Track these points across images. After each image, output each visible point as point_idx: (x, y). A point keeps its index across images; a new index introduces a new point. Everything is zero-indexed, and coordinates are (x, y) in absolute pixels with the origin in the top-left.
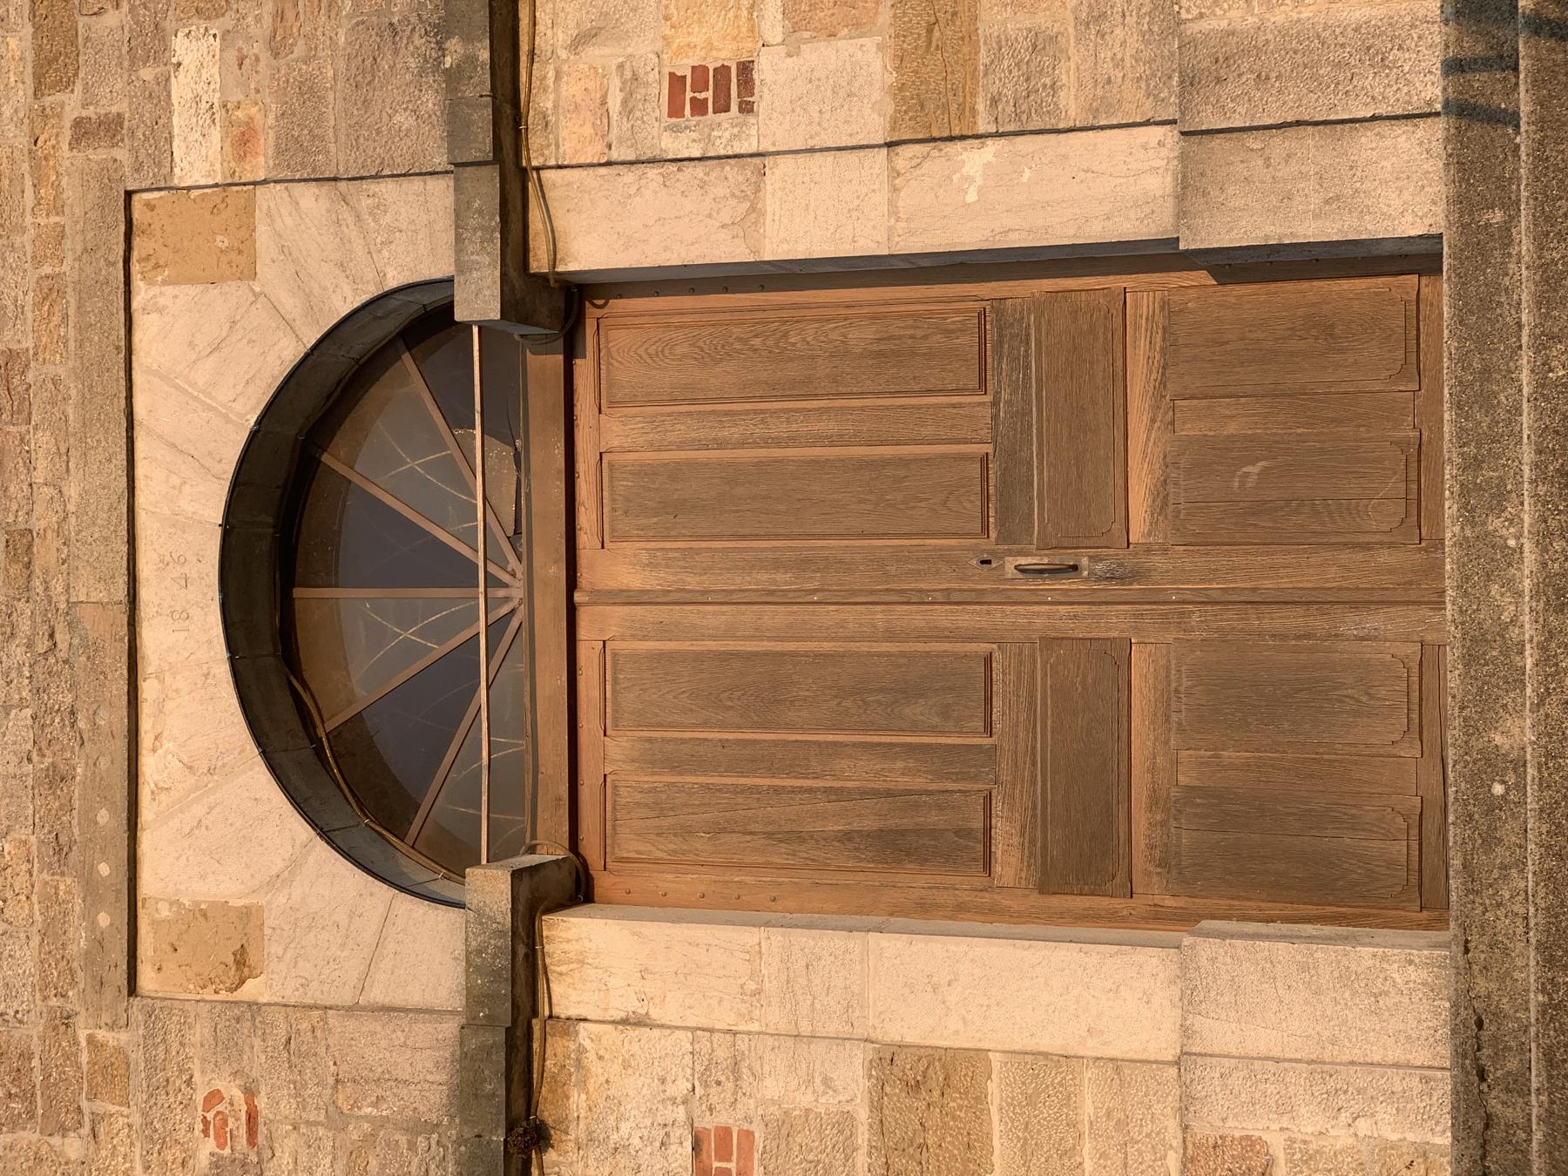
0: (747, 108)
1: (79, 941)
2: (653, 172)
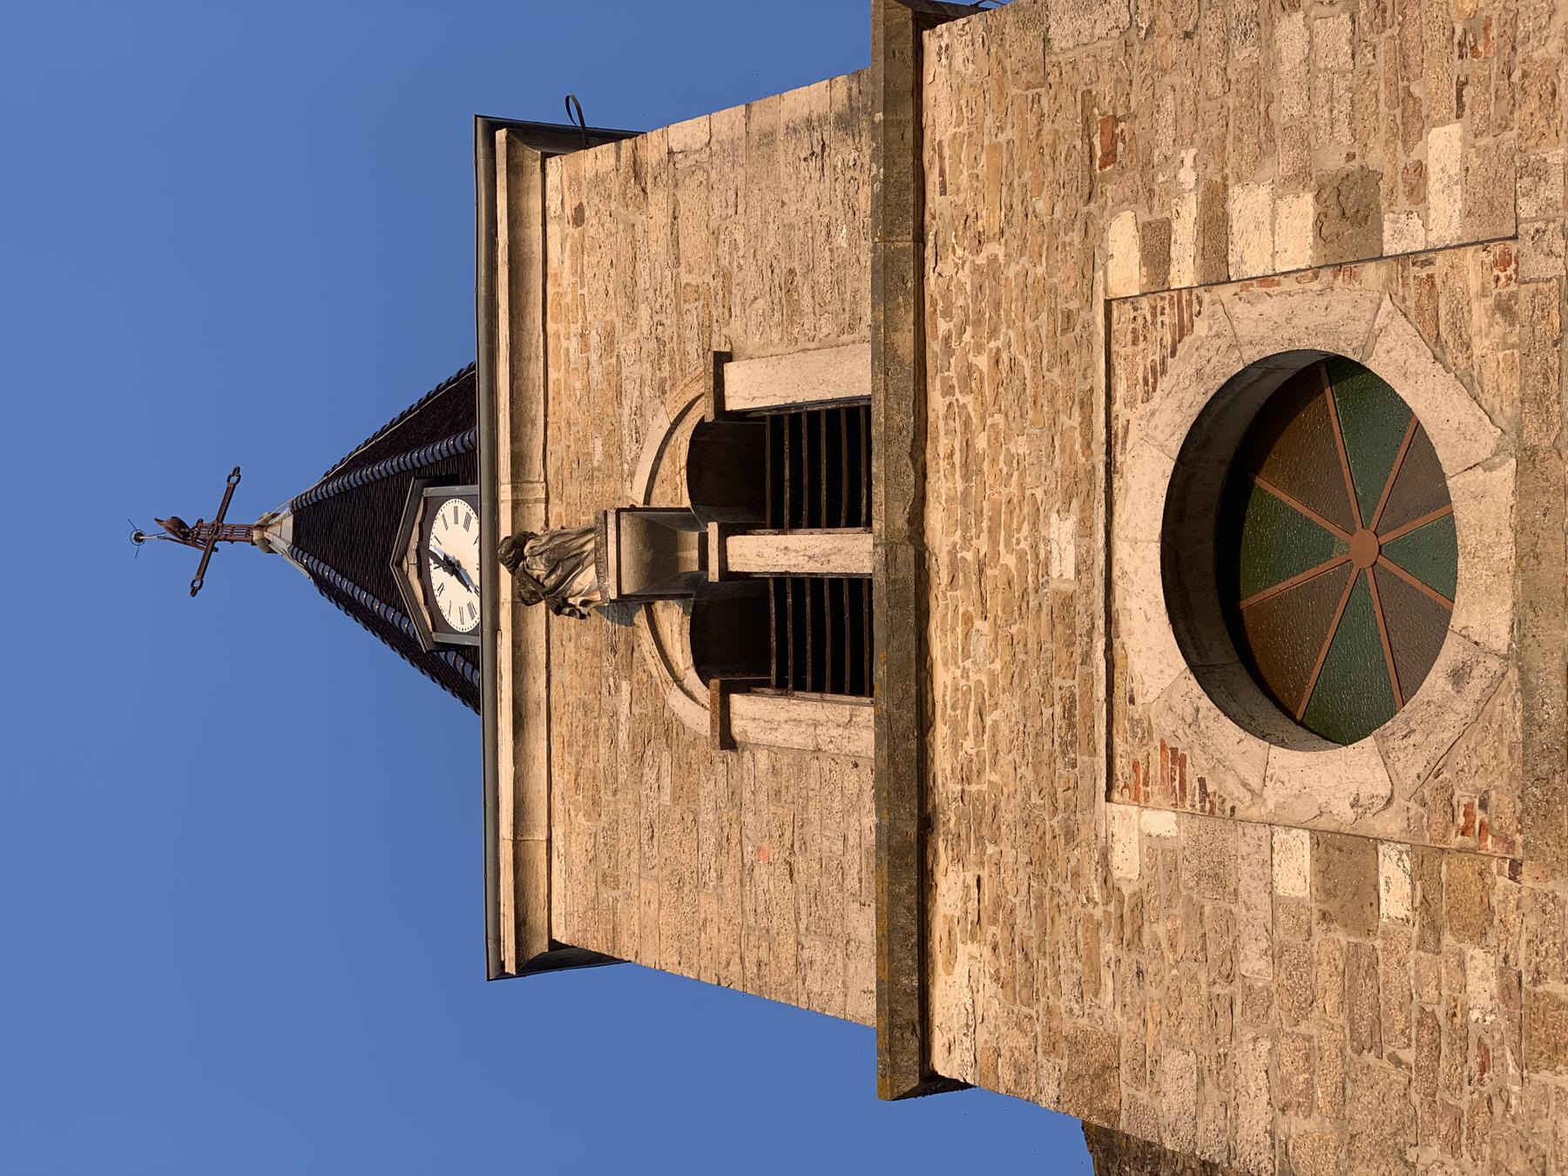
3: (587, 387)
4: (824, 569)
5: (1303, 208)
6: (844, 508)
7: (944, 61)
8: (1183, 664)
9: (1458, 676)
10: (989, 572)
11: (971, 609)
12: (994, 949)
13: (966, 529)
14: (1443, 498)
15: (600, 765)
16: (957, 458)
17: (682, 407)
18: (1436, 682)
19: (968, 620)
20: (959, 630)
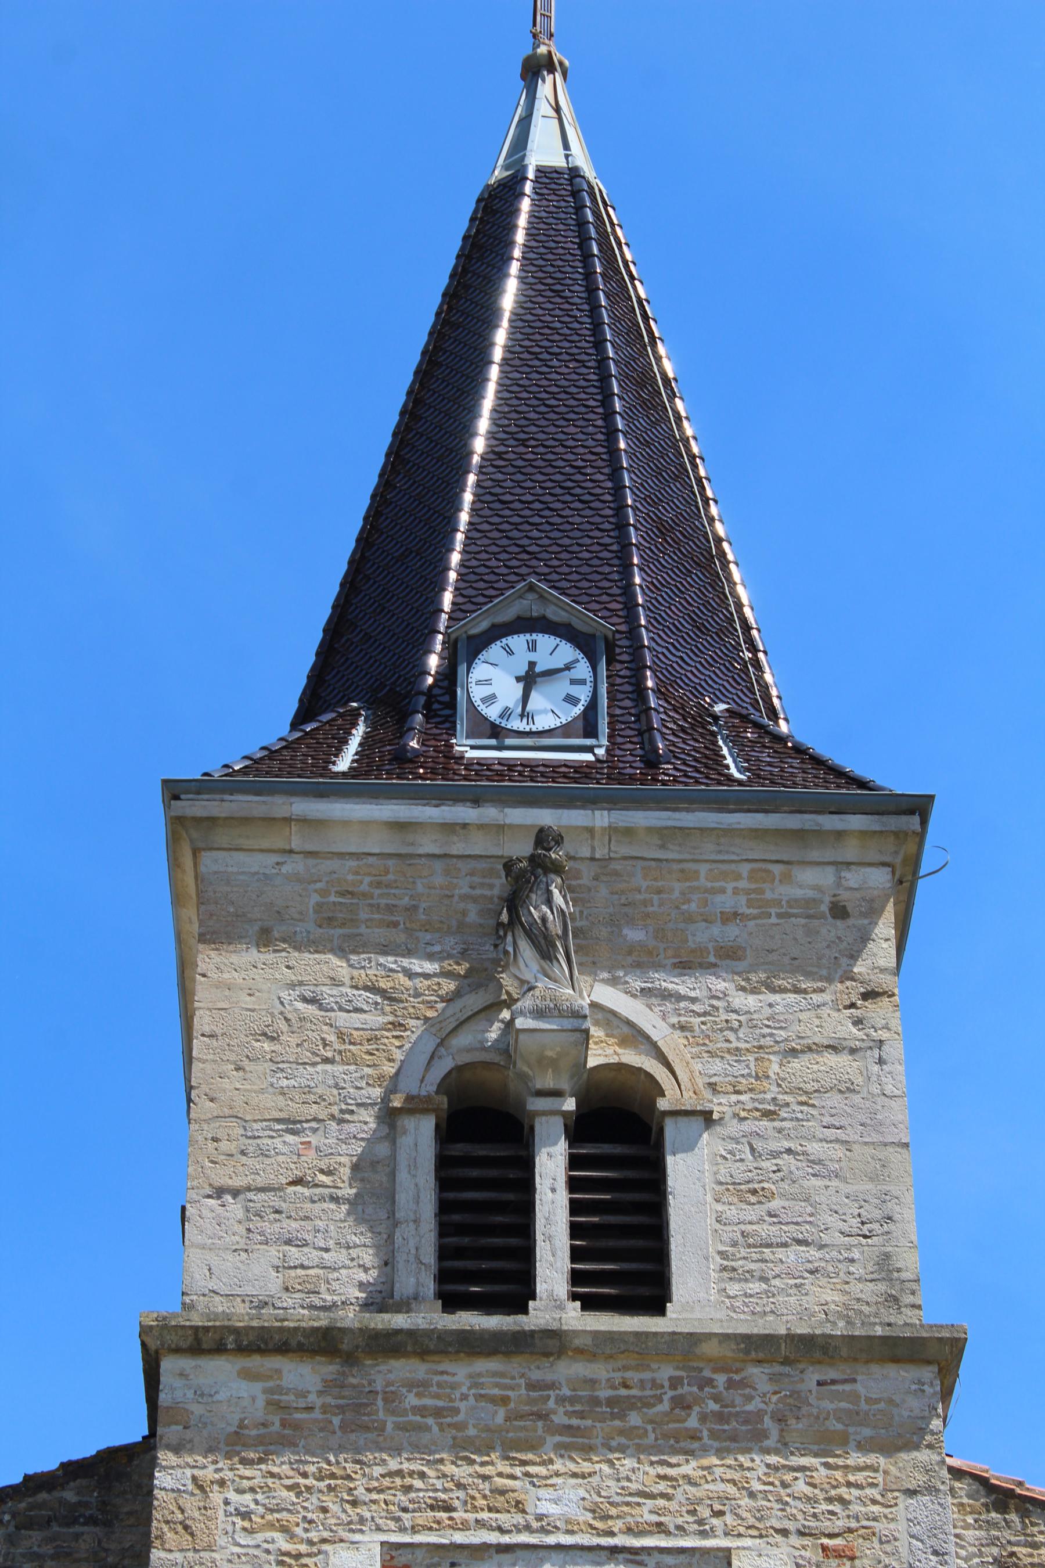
3: (690, 919)
4: (539, 1237)
7: (914, 1387)
10: (540, 1424)
11: (512, 1405)
12: (263, 1424)
13: (573, 1400)
15: (363, 929)
16: (623, 1392)
17: (670, 1058)
19: (505, 1401)
20: (496, 1391)
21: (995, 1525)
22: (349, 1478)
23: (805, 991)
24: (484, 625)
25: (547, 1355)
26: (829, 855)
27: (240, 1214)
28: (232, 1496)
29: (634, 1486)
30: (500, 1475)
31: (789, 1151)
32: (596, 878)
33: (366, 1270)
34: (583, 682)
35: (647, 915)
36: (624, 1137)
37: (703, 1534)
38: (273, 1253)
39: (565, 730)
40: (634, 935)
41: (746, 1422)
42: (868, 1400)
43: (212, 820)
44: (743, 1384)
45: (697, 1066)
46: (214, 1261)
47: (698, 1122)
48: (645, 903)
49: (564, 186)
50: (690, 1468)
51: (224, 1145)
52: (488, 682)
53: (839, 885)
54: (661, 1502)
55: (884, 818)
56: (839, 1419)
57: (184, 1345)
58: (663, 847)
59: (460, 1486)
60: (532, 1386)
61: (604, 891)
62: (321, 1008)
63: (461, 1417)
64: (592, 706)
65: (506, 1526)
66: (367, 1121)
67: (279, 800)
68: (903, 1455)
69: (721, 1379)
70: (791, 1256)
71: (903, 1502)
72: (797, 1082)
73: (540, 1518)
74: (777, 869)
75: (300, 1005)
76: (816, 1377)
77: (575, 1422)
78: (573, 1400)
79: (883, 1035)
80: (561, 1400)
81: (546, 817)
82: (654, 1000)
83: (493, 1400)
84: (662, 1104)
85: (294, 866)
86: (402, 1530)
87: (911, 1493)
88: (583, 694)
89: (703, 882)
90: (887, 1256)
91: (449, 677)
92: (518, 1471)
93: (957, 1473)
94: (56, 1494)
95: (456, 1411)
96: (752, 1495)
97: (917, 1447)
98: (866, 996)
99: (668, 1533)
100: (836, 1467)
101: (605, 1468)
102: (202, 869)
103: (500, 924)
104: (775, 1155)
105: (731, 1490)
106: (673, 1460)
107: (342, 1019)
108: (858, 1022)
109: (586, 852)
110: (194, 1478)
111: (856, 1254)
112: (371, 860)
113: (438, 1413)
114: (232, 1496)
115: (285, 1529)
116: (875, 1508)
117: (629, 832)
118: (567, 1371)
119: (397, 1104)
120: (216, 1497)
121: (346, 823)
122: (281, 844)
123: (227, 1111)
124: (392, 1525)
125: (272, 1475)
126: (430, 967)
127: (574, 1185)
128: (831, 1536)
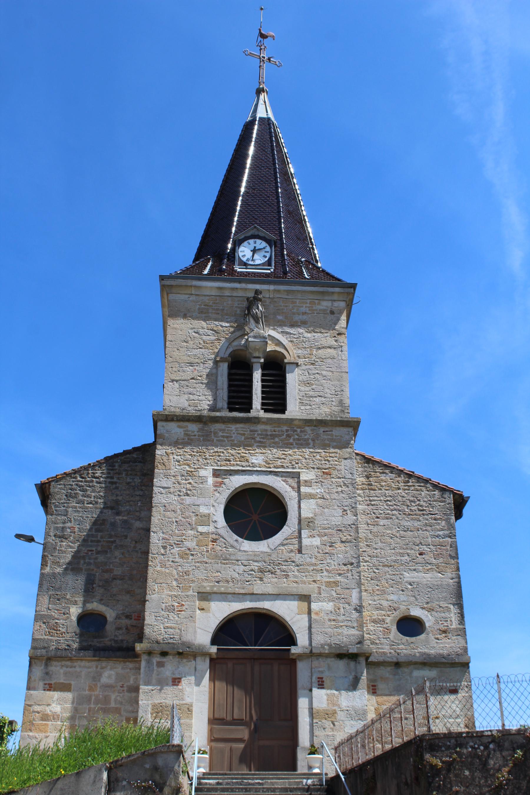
0: (318, 688)
1: (205, 584)
2: (310, 674)
3: (294, 314)
4: (254, 394)
5: (311, 515)
6: (266, 407)
8: (237, 487)
9: (236, 541)
13: (261, 435)
14: (265, 539)
16: (274, 433)
18: (236, 537)
19: (244, 434)
20: (242, 432)
21: (366, 467)
22: (204, 453)
23: (323, 333)
24: (243, 237)
25: (255, 423)
26: (330, 298)
27: (178, 387)
28: (175, 457)
29: (276, 456)
30: (243, 453)
31: (318, 373)
32: (270, 303)
33: (210, 401)
34: (268, 252)
35: (283, 313)
36: (276, 369)
37: (293, 468)
38: (186, 396)
39: (263, 264)
40: (280, 317)
41: (305, 441)
42: (336, 436)
43: (172, 286)
44: (304, 431)
45: (295, 351)
46: (171, 398)
47: (295, 366)
48: (283, 309)
49: (266, 122)
50: (290, 452)
51: (174, 369)
52: (244, 251)
53: (332, 306)
54: (283, 460)
55: (345, 289)
56: (328, 440)
57: (163, 419)
58: (287, 295)
59: (232, 455)
60: (251, 431)
61: (272, 306)
62: (199, 334)
63: (233, 438)
64: (270, 258)
65: (244, 465)
66: (210, 364)
67: (189, 281)
68: (344, 450)
69: (299, 430)
70: (317, 400)
71: (343, 461)
72: (320, 356)
73: (252, 463)
74: (317, 301)
75: (194, 334)
76: (323, 430)
77: (262, 440)
78: (261, 435)
79: (342, 344)
80: (258, 435)
81: (258, 287)
82: (284, 334)
83: (241, 434)
84: (286, 361)
85: (193, 298)
86: (218, 466)
87: (345, 459)
88: (268, 255)
89: (297, 304)
90: (342, 400)
91: (234, 250)
92: (247, 452)
93: (357, 454)
94: (131, 455)
95: (232, 437)
96: (306, 459)
97: (347, 448)
98: (338, 334)
99: (284, 468)
100: (327, 452)
101: (269, 452)
102: (169, 298)
103: (245, 314)
104: (314, 374)
105: (300, 457)
106: (286, 450)
107: (205, 338)
108: (336, 341)
109: (267, 296)
110: (166, 452)
111: (334, 400)
112: (213, 297)
113: (227, 437)
114: (175, 457)
115: (188, 465)
116: (336, 463)
117: (279, 291)
118: (260, 427)
119: (218, 359)
120: (171, 457)
121: (206, 287)
122: (189, 292)
123: (175, 360)
124: (215, 464)
125: (185, 452)
126: (227, 325)
127: (263, 381)
128: (325, 469)
